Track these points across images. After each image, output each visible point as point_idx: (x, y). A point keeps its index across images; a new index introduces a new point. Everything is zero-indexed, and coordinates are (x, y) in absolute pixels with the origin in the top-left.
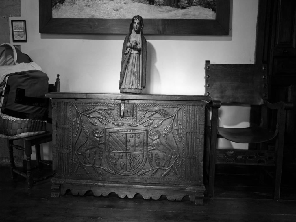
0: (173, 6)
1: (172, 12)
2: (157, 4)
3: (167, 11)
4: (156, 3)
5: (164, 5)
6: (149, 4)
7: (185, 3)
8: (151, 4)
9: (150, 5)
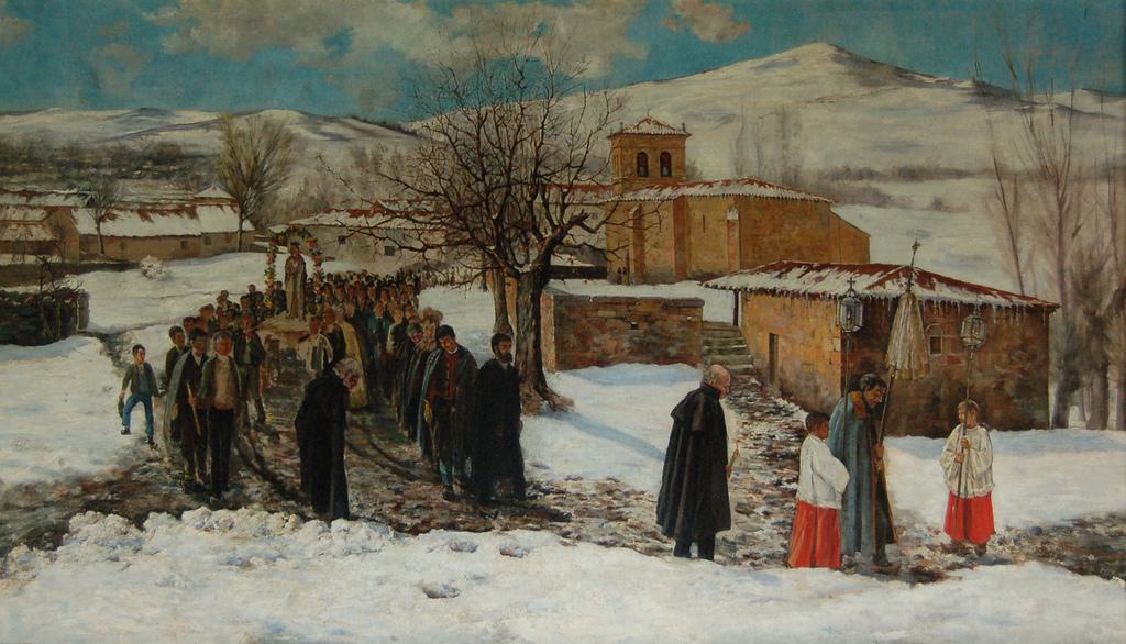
0: (850, 567)
1: (841, 601)
2: (739, 554)
3: (811, 598)
4: (732, 546)
5: (784, 561)
6: (682, 551)
7: (931, 547)
8: (695, 554)
9: (684, 559)
